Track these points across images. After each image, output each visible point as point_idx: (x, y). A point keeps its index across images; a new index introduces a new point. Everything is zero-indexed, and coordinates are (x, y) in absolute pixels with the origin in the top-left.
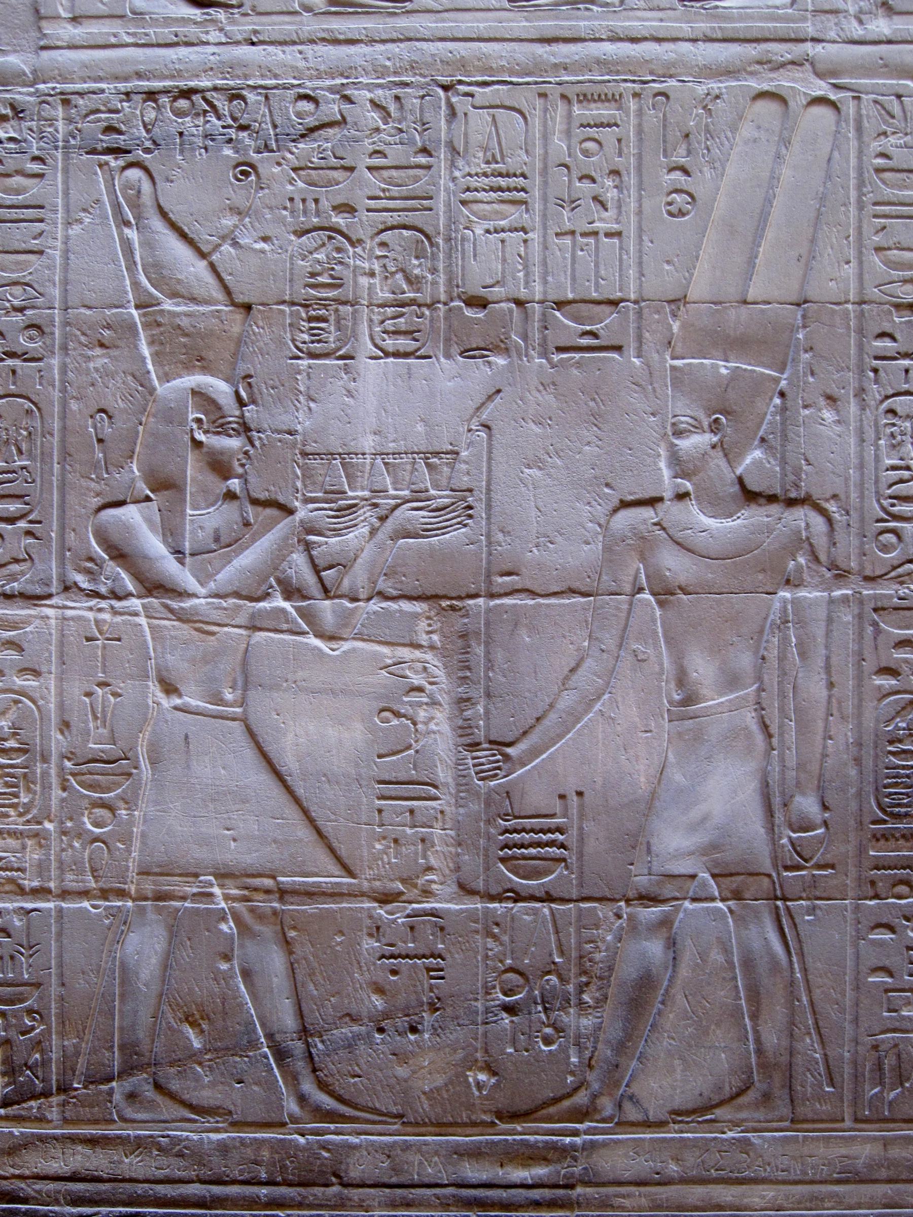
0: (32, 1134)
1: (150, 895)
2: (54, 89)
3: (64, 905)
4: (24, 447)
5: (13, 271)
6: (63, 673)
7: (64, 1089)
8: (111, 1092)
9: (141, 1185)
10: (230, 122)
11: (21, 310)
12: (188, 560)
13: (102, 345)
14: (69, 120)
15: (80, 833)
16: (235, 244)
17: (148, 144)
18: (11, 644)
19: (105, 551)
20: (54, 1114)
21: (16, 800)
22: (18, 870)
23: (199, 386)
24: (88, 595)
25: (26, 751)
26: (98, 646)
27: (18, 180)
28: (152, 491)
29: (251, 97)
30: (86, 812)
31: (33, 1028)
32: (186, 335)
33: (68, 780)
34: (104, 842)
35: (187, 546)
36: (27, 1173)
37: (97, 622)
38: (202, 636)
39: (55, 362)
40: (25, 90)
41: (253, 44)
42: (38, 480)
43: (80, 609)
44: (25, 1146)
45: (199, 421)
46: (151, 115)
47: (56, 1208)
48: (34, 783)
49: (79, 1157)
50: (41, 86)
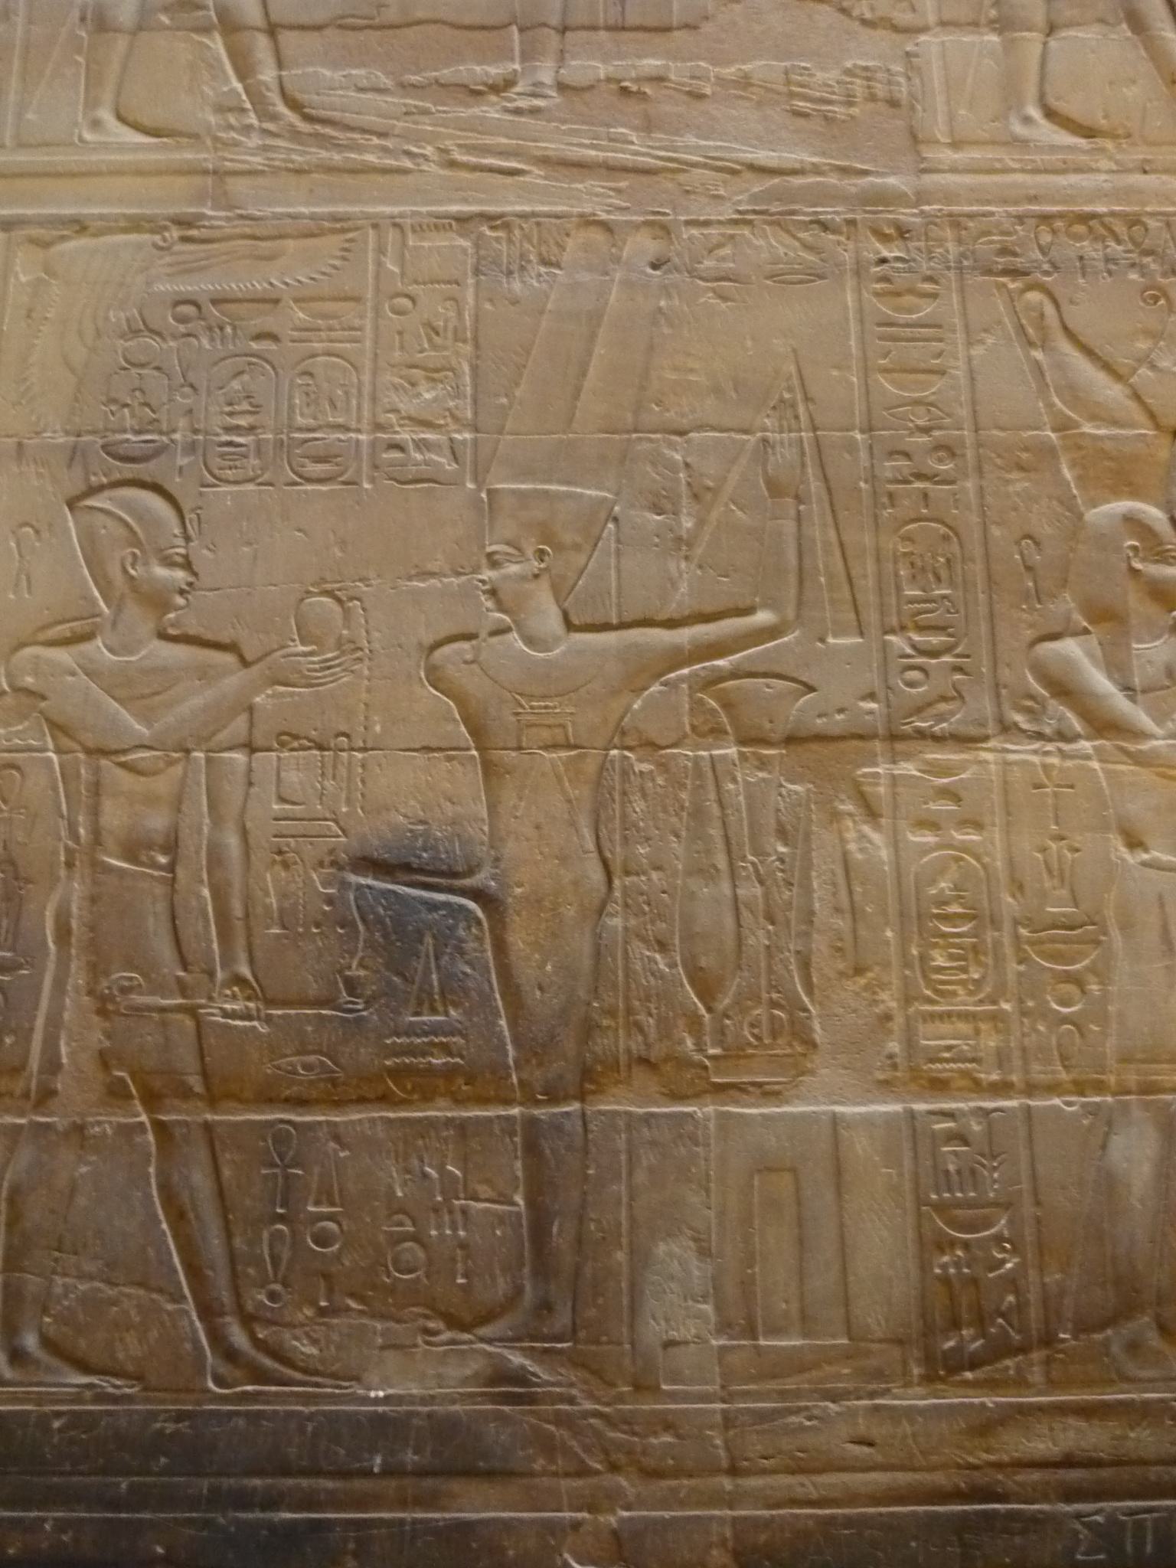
0: (1010, 1405)
1: (1134, 1088)
2: (940, 210)
3: (1031, 1103)
4: (944, 574)
5: (913, 391)
6: (1008, 824)
7: (1048, 1340)
8: (1106, 1344)
9: (1154, 1469)
10: (1130, 246)
11: (926, 430)
12: (1140, 697)
13: (1021, 468)
14: (960, 241)
15: (1045, 1013)
16: (1153, 367)
17: (1046, 267)
18: (946, 793)
19: (1045, 688)
20: (1036, 1376)
21: (964, 976)
22: (973, 1060)
23: (1130, 511)
24: (1030, 737)
25: (974, 917)
26: (1046, 794)
27: (908, 300)
28: (1090, 623)
29: (1152, 223)
30: (1049, 988)
31: (1003, 1262)
32: (1111, 459)
33: (1025, 951)
34: (1074, 1024)
35: (1137, 681)
36: (1006, 1458)
37: (1045, 766)
38: (1165, 781)
39: (970, 485)
40: (908, 211)
41: (1145, 172)
42: (962, 611)
43: (1023, 752)
44: (1002, 1422)
45: (1134, 548)
46: (1046, 238)
47: (1046, 1507)
48: (985, 954)
49: (1071, 1434)
50: (926, 208)
